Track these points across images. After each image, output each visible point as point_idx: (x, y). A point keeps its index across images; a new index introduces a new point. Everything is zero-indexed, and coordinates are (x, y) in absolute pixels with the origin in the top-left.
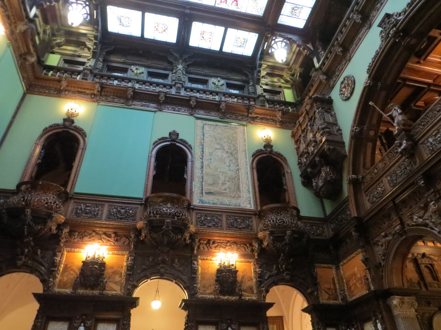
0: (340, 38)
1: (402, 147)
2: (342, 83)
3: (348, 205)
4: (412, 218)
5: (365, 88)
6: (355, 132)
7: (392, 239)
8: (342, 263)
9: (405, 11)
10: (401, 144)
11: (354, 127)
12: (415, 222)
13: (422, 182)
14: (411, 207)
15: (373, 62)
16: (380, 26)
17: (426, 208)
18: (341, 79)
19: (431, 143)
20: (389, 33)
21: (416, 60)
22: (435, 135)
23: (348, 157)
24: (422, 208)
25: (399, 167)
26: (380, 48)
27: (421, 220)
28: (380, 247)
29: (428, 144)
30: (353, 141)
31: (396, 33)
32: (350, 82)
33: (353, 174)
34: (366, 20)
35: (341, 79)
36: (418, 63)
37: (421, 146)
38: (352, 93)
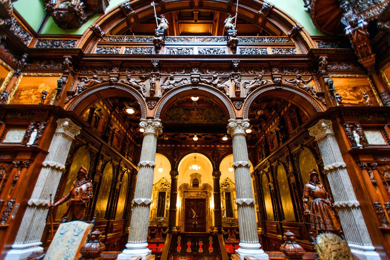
1: (159, 38)
3: (76, 41)
4: (129, 79)
6: (126, 6)
7: (100, 83)
8: (26, 74)
10: (158, 36)
11: (127, 2)
12: (131, 83)
13: (157, 64)
14: (134, 73)
17: (143, 79)
19: (173, 52)
21: (177, 18)
23: (104, 15)
24: (141, 78)
25: (142, 48)
28: (84, 83)
29: (172, 51)
30: (118, 10)
33: (100, 26)
36: (176, 21)
37: (166, 49)
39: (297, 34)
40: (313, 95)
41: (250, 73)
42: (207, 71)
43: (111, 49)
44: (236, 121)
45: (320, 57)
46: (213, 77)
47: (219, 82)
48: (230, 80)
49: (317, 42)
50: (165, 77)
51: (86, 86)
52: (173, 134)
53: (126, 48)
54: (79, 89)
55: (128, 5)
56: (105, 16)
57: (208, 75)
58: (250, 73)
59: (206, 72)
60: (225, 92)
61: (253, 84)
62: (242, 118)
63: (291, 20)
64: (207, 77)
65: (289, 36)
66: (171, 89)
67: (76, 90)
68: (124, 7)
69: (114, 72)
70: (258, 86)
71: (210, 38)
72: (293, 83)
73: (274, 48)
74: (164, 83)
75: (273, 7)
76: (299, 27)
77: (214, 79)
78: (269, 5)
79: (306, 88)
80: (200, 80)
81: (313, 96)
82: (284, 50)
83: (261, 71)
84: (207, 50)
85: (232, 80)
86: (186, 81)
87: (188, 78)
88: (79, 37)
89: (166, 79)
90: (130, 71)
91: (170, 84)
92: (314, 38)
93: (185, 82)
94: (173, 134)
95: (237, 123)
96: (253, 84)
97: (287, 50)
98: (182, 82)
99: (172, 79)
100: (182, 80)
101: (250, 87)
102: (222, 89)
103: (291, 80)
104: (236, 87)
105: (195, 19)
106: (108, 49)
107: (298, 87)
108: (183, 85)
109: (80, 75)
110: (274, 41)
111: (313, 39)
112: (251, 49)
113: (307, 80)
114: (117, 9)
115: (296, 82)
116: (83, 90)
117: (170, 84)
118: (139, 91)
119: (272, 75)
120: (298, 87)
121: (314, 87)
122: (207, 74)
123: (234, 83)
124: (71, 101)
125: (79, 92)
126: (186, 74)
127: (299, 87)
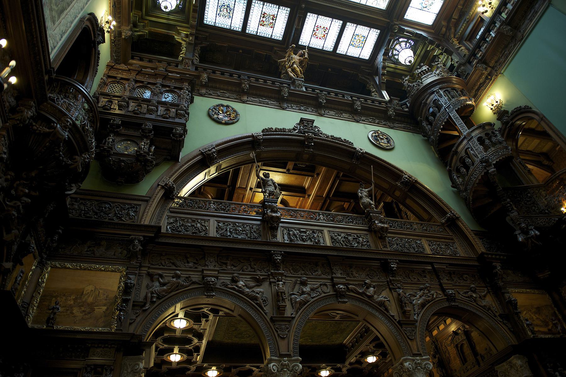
0: (218, 76)
2: (222, 106)
5: (252, 136)
9: (328, 137)
12: (240, 288)
15: (276, 131)
16: (302, 120)
17: (259, 282)
18: (225, 103)
19: (294, 234)
20: (307, 132)
22: (301, 232)
26: (290, 130)
27: (248, 290)
28: (158, 284)
30: (199, 157)
31: (312, 138)
32: (233, 115)
34: (281, 100)
35: (225, 103)
38: (226, 124)
39: (452, 223)
40: (496, 316)
41: (413, 279)
42: (354, 273)
43: (194, 221)
44: (414, 360)
45: (494, 264)
46: (366, 283)
47: (375, 292)
48: (388, 289)
49: (480, 239)
50: (293, 279)
51: (164, 291)
52: (228, 365)
53: (219, 222)
54: (152, 297)
55: (214, 152)
56: (181, 167)
57: (355, 279)
58: (413, 279)
59: (352, 274)
60: (388, 312)
61: (420, 297)
62: (420, 355)
63: (443, 203)
64: (357, 283)
65: (443, 224)
66: (308, 301)
67: (146, 297)
68: (209, 155)
69: (210, 268)
70: (429, 302)
71: (341, 215)
72: (468, 297)
73: (430, 241)
74: (293, 289)
75: (416, 182)
76: (455, 215)
77: (368, 288)
78: (410, 178)
79: (485, 306)
80: (348, 288)
81: (496, 318)
82: (443, 245)
83: (425, 277)
84: (343, 235)
85: (390, 289)
86: (325, 287)
87: (328, 282)
88: (146, 200)
89: (295, 283)
90: (235, 267)
91: (303, 293)
92: (477, 233)
93: (325, 289)
94: (228, 365)
95: (415, 363)
96: (420, 297)
97: (446, 245)
98: (319, 290)
99: (304, 284)
100: (321, 285)
101: (419, 302)
102: (382, 304)
103: (466, 293)
104: (401, 303)
105: (287, 168)
106: (188, 222)
107: (475, 304)
108: (323, 295)
109: (149, 268)
110: (426, 230)
111: (475, 235)
112: (401, 239)
113: (483, 294)
114: (197, 156)
115: (472, 296)
116: (159, 298)
117: (303, 293)
118: (257, 304)
119: (441, 285)
120: (475, 304)
121: (494, 305)
122: (355, 277)
123: (395, 294)
124: (138, 319)
125: (153, 303)
126: (323, 276)
127: (477, 304)
